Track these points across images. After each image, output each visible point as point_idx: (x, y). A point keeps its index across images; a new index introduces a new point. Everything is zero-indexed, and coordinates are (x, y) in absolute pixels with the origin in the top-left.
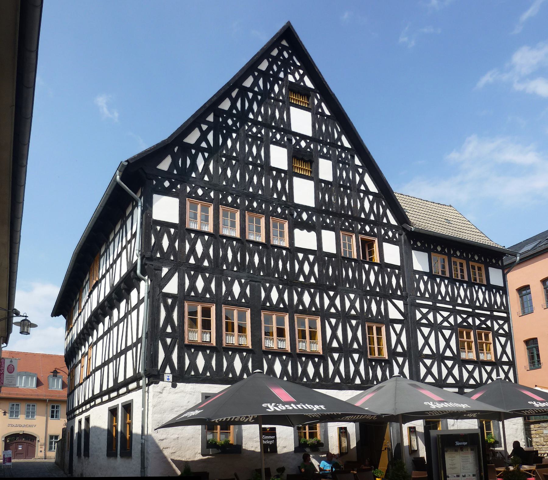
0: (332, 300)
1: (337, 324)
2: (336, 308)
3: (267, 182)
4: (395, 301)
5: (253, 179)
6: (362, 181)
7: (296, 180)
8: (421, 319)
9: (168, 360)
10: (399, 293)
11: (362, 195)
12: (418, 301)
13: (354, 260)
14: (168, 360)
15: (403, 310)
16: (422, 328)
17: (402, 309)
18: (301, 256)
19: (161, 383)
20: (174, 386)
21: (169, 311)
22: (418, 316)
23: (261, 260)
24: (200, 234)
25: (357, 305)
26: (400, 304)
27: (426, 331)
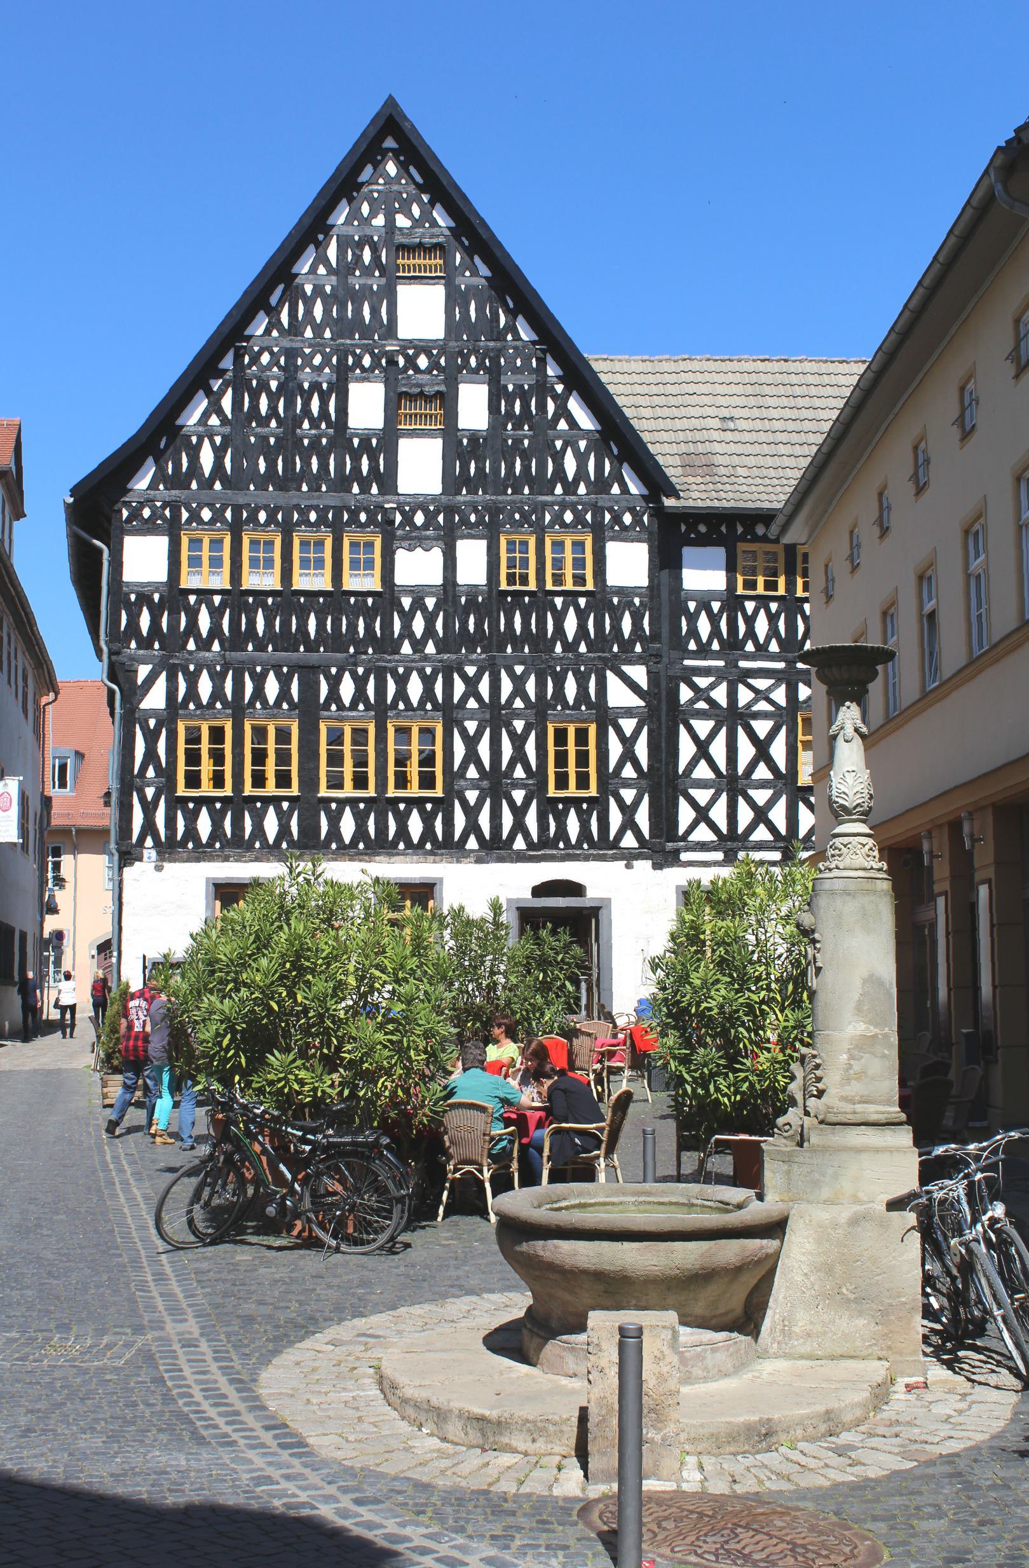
0: (472, 684)
1: (479, 733)
2: (479, 699)
3: (340, 465)
4: (627, 669)
5: (310, 464)
6: (563, 412)
7: (404, 444)
8: (692, 701)
9: (149, 826)
10: (638, 648)
11: (559, 444)
12: (687, 662)
13: (530, 594)
14: (149, 826)
15: (645, 686)
16: (692, 722)
17: (643, 683)
18: (406, 602)
19: (137, 864)
20: (159, 868)
21: (151, 738)
22: (685, 694)
23: (321, 625)
24: (204, 594)
25: (531, 687)
26: (639, 673)
27: (703, 727)
